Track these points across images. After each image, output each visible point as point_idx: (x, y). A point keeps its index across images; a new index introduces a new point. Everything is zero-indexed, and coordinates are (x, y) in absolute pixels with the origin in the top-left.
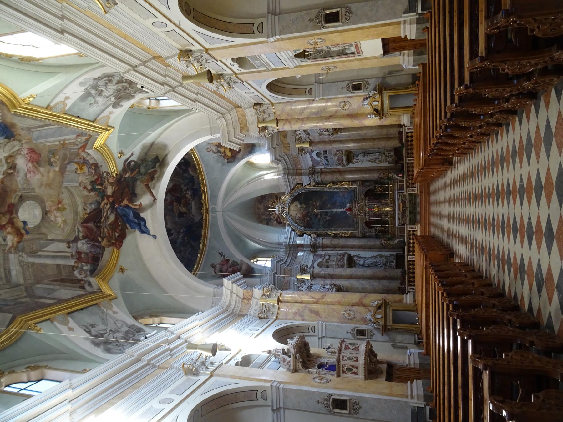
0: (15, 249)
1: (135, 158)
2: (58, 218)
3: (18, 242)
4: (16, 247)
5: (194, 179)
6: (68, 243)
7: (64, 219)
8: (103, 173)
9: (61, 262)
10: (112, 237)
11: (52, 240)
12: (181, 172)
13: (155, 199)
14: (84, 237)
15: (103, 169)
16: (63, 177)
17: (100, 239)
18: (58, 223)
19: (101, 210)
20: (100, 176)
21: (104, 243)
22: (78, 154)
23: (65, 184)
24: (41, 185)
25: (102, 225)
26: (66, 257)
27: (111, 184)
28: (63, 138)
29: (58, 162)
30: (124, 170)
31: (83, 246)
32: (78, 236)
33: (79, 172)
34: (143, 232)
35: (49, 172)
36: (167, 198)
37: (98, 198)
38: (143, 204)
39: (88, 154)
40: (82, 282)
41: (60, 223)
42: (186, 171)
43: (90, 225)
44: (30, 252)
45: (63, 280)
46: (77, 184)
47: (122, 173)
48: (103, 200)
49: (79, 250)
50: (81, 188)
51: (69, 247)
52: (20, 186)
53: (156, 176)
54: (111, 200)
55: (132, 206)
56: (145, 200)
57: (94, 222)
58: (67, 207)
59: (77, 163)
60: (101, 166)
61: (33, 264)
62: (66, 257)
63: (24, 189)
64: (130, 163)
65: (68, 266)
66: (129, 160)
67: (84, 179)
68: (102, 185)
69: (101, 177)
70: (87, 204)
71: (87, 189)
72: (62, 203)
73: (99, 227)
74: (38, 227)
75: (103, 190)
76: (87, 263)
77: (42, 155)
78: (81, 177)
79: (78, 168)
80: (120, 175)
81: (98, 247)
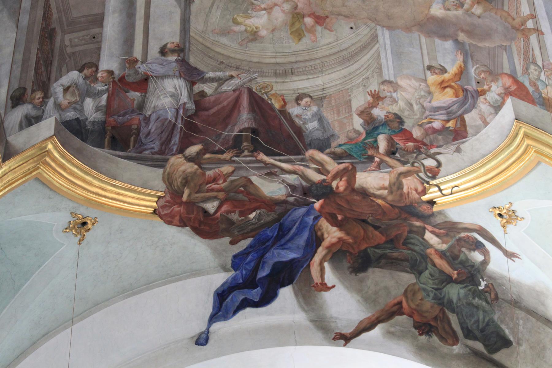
1: (497, 264)
6: (180, 50)
7: (263, 33)
8: (433, 156)
9: (111, 27)
13: (345, 339)
14: (199, 99)
15: (447, 156)
16: (408, 29)
17: (193, 150)
18: (251, 17)
19: (298, 152)
20: (422, 147)
21: (180, 165)
22: (494, 74)
23: (385, 37)
25: (246, 156)
26: (128, 42)
27: (396, 186)
28: (545, 25)
29: (460, 12)
30: (450, 229)
31: (168, 96)
32: (204, 80)
33: (432, 78)
34: (221, 295)
37: (342, 140)
38: (326, 295)
39: (497, 108)
40: (39, 95)
41: (249, 22)
43: (245, 119)
45: (48, 35)
46: (389, 73)
47: (439, 220)
48: (337, 157)
49: (151, 85)
50: (374, 87)
51: (163, 51)
53: (435, 338)
54: (339, 185)
55: (317, 258)
56: (343, 302)
57: (254, 131)
58: (306, 41)
59: (461, 73)
60: (458, 150)
62: (128, 42)
64: (478, 246)
65: (99, 49)
66: (488, 245)
68: (391, 152)
69: (418, 150)
70: (320, 106)
71: (372, 106)
72: (319, 28)
73: (236, 144)
75: (371, 159)
76: (108, 110)
78: (415, 83)
79: (446, 76)
80: (433, 215)
81: (167, 142)
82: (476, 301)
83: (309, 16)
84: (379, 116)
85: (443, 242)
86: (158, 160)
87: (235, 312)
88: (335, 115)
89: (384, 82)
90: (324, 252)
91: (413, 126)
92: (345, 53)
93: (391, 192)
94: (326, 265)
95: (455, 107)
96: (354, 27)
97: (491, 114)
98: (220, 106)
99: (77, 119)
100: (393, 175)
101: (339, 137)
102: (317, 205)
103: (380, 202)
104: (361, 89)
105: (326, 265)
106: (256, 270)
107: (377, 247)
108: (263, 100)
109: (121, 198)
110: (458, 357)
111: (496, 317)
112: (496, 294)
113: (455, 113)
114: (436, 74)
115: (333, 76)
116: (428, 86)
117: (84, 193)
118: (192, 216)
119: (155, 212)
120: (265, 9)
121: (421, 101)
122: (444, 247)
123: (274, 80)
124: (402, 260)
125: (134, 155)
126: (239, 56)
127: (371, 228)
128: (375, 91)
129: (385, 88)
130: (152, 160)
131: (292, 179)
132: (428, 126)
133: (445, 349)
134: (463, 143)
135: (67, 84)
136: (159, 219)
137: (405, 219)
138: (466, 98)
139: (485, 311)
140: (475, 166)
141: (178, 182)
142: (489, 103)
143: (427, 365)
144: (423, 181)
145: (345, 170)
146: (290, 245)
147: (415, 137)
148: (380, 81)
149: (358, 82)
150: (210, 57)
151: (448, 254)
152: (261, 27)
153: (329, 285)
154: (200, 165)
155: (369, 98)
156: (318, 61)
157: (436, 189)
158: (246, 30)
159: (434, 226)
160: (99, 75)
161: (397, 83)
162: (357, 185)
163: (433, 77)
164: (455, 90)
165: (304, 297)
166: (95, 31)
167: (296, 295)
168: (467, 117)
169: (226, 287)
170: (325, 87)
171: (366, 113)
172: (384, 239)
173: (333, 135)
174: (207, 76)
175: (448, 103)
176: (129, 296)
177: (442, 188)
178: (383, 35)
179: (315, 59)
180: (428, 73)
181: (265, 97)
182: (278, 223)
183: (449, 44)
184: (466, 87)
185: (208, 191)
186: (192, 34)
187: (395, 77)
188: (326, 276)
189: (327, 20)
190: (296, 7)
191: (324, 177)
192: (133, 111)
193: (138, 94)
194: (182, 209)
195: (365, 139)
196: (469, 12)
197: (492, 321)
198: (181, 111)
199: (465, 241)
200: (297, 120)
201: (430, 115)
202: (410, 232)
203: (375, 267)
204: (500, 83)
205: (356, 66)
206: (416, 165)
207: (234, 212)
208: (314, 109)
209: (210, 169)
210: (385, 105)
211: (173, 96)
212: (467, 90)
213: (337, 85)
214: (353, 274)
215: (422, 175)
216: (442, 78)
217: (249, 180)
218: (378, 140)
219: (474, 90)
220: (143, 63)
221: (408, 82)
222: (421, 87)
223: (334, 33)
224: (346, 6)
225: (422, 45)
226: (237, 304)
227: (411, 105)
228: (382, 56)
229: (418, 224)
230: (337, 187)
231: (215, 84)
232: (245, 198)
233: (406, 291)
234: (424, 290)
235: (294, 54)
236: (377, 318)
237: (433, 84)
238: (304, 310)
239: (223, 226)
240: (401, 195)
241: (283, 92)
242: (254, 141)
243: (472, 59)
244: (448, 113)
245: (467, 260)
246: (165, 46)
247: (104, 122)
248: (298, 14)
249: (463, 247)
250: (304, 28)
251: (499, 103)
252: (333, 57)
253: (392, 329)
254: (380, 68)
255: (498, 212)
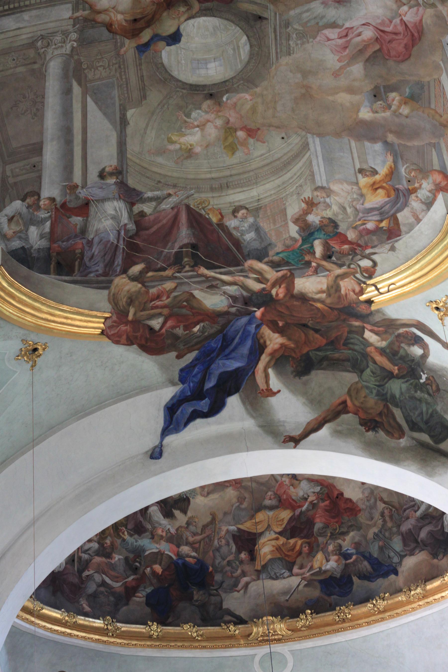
0: (86, 20)
2: (201, 132)
3: (109, 26)
4: (94, 20)
5: (386, 575)
6: (118, 172)
7: (198, 149)
8: (368, 257)
9: (51, 155)
10: (144, 310)
11: (124, 122)
12: (406, 527)
13: (295, 441)
14: (139, 219)
15: (382, 255)
16: (338, 135)
17: (136, 269)
18: (185, 135)
19: (237, 263)
20: (357, 249)
21: (124, 285)
22: (424, 172)
23: (315, 144)
24: (305, 74)
25: (187, 272)
26: (68, 168)
27: (333, 289)
29: (388, 114)
30: (388, 326)
31: (109, 218)
32: (143, 201)
33: (363, 181)
34: (171, 409)
35: (351, 90)
36: (304, 485)
37: (279, 248)
38: (273, 400)
39: (429, 204)
41: (183, 140)
42: (412, 542)
43: (184, 235)
44: (79, 63)
46: (321, 179)
47: (377, 318)
48: (275, 265)
49: (92, 209)
50: (307, 194)
51: (102, 175)
52: (292, 13)
53: (381, 433)
54: (279, 292)
55: (261, 366)
56: (289, 406)
57: (194, 246)
58: (240, 154)
59: (392, 173)
60: (393, 249)
61: (40, 76)
62: (68, 168)
63: (287, 24)
64: (417, 341)
65: (40, 177)
66: (427, 339)
67: (341, 200)
68: (327, 257)
69: (353, 252)
71: (306, 212)
72: (251, 141)
73: (177, 260)
74: (165, 78)
75: (308, 264)
76: (52, 236)
77: (404, 66)
79: (378, 177)
80: (371, 314)
81: (110, 264)
82: (419, 394)
83: (241, 129)
84: (314, 222)
85: (382, 340)
86: (102, 282)
87: (186, 424)
88: (271, 224)
89: (317, 188)
90: (267, 359)
91: (348, 229)
92: (278, 162)
93: (329, 295)
94: (270, 371)
95: (387, 207)
96: (285, 137)
97: (423, 210)
98: (160, 224)
99: (23, 248)
100: (330, 279)
101: (276, 246)
102: (258, 314)
103: (319, 305)
104: (295, 197)
105: (270, 371)
106: (203, 381)
107: (319, 349)
108: (201, 215)
109: (69, 321)
110: (406, 449)
111: (439, 408)
112: (438, 386)
113: (388, 213)
114: (367, 176)
115: (268, 186)
116: (360, 189)
117: (33, 320)
118: (138, 334)
119: (103, 333)
120: (198, 126)
121: (354, 203)
122: (384, 344)
123: (210, 195)
124: (343, 361)
125: (79, 278)
126: (175, 174)
127: (311, 332)
128: (309, 198)
129: (319, 194)
130: (98, 282)
131: (232, 290)
132: (362, 228)
133: (392, 443)
134: (397, 241)
135: (11, 215)
136: (107, 339)
137: (344, 320)
138: (398, 197)
139: (427, 403)
140: (410, 263)
141: (123, 301)
142: (421, 200)
143: (376, 459)
144: (360, 282)
145: (284, 277)
146: (233, 354)
147: (349, 239)
148: (313, 187)
149: (291, 190)
150: (148, 177)
151: (388, 351)
152: (195, 144)
153: (275, 390)
154: (143, 284)
155: (304, 205)
156: (251, 174)
157: (373, 288)
158: (181, 149)
159: (374, 325)
160: (42, 203)
161: (329, 189)
162: (296, 291)
163: (364, 179)
164: (387, 190)
165: (252, 404)
166: (34, 160)
167: (244, 403)
168: (400, 216)
169: (175, 400)
170: (260, 198)
171: (299, 219)
172: (324, 341)
173: (270, 244)
174: (146, 196)
175: (380, 204)
176: (82, 417)
177: (379, 286)
178: (314, 142)
179: (249, 172)
180: (360, 176)
181: (203, 212)
182: (221, 335)
183: (378, 146)
184: (397, 186)
185: (153, 308)
186: (129, 156)
187: (328, 182)
188: (271, 382)
189: (259, 132)
190: (228, 122)
191: (263, 286)
192: (76, 236)
193: (80, 219)
194: (128, 328)
195: (301, 246)
196: (397, 113)
197: (435, 411)
198: (122, 233)
199: (404, 336)
200: (234, 233)
201: (364, 217)
202: (350, 332)
203: (318, 369)
204: (430, 180)
205: (289, 175)
206: (352, 266)
207: (179, 326)
208: (251, 220)
209: (153, 287)
210: (319, 210)
211: (114, 218)
212: (398, 190)
213: (271, 195)
214: (297, 378)
215: (358, 276)
216: (374, 180)
217: (192, 295)
218: (315, 245)
219: (405, 189)
220: (82, 188)
221: (341, 186)
222: (353, 190)
223: (266, 144)
224: (276, 117)
225: (353, 150)
226: (187, 416)
227: (345, 209)
228: (314, 163)
229: (357, 324)
230: (277, 294)
231: (154, 203)
232: (188, 312)
233: (349, 390)
234: (367, 387)
235: (228, 168)
236: (324, 419)
237: (365, 186)
238: (252, 416)
239: (169, 341)
240: (340, 297)
241: (219, 206)
242: (194, 256)
243: (402, 159)
244: (381, 214)
245: (407, 355)
246: (104, 169)
247: (49, 249)
248: (229, 128)
249: (402, 342)
250: (236, 142)
251: (431, 199)
252: (266, 168)
253: (339, 428)
254: (312, 175)
255: (434, 306)
